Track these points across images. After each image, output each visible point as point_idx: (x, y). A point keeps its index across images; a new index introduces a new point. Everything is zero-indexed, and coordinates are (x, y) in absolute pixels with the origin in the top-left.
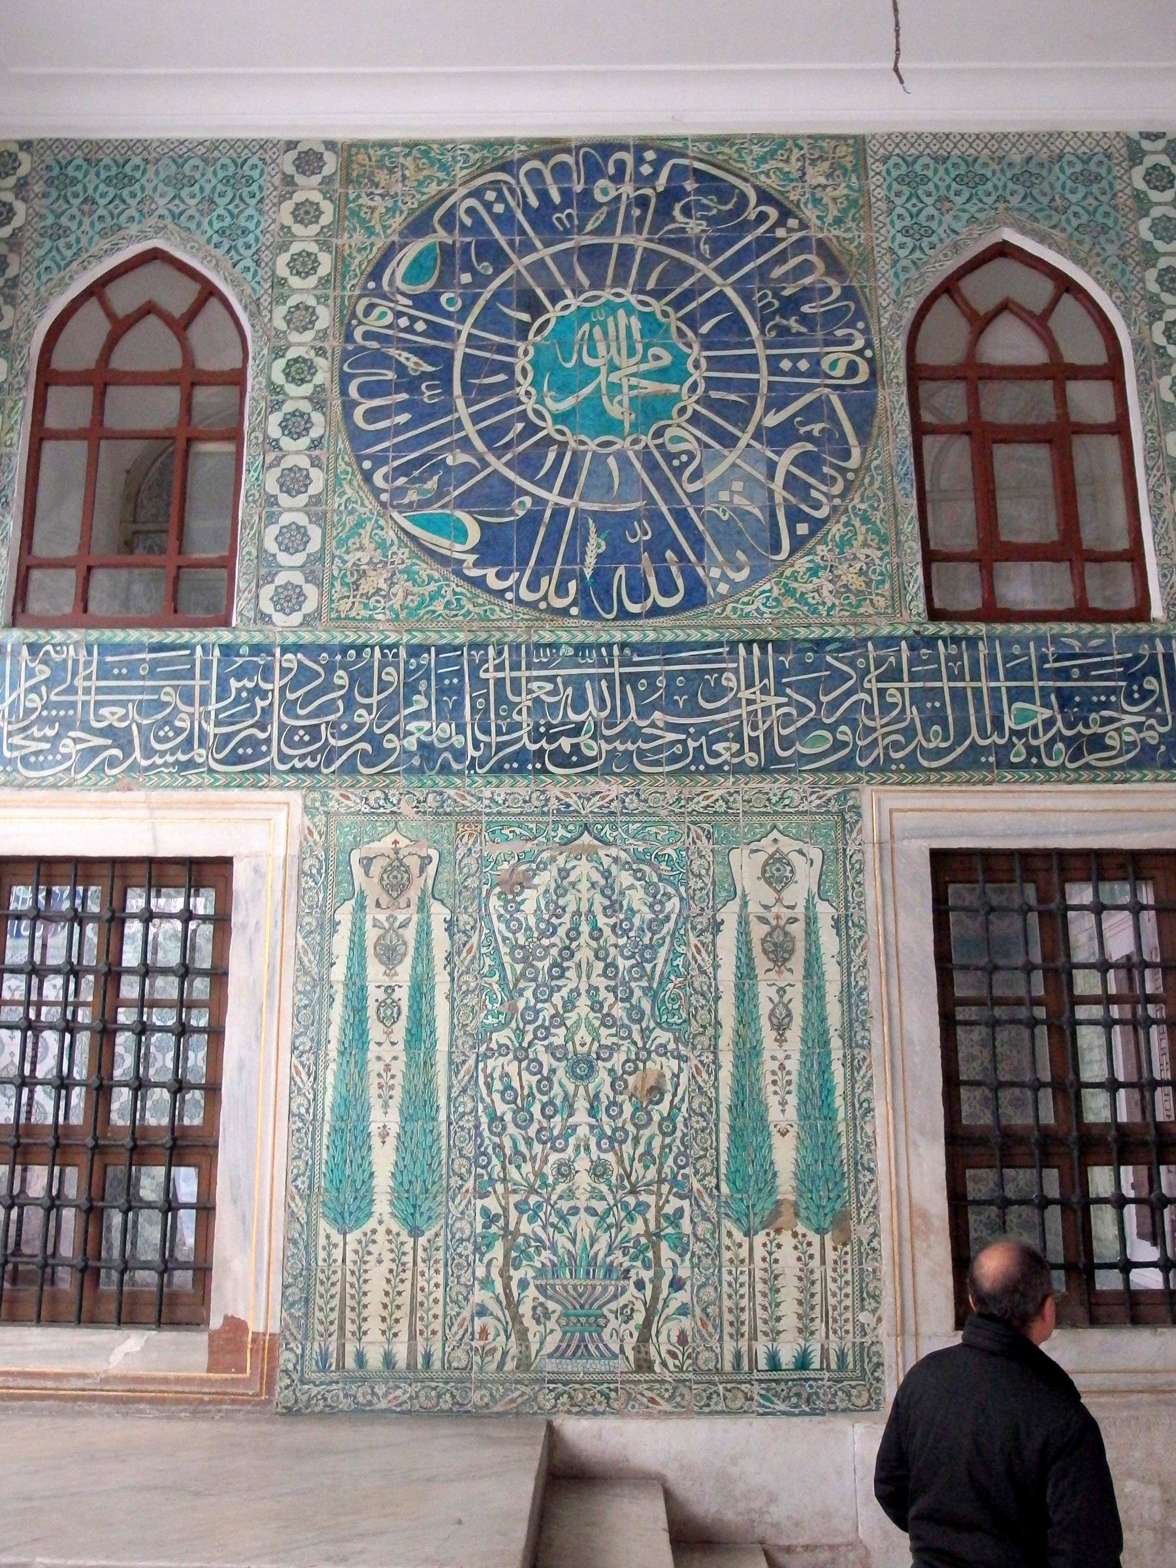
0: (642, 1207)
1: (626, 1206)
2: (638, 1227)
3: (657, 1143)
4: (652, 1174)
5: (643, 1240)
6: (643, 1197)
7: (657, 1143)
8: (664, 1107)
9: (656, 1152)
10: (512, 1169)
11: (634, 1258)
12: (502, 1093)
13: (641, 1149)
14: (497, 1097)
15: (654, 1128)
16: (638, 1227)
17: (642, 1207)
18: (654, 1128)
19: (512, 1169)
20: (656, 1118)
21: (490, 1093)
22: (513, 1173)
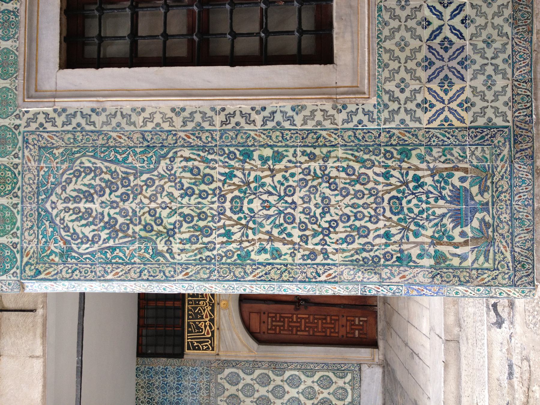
0: (416, 179)
1: (416, 188)
2: (429, 180)
3: (377, 170)
4: (396, 173)
5: (436, 178)
6: (410, 178)
7: (377, 170)
8: (356, 166)
9: (383, 170)
10: (393, 239)
11: (446, 183)
12: (349, 244)
13: (381, 179)
14: (351, 247)
15: (370, 172)
16: (429, 180)
17: (416, 179)
18: (370, 172)
19: (393, 239)
20: (363, 170)
21: (350, 251)
22: (397, 238)
